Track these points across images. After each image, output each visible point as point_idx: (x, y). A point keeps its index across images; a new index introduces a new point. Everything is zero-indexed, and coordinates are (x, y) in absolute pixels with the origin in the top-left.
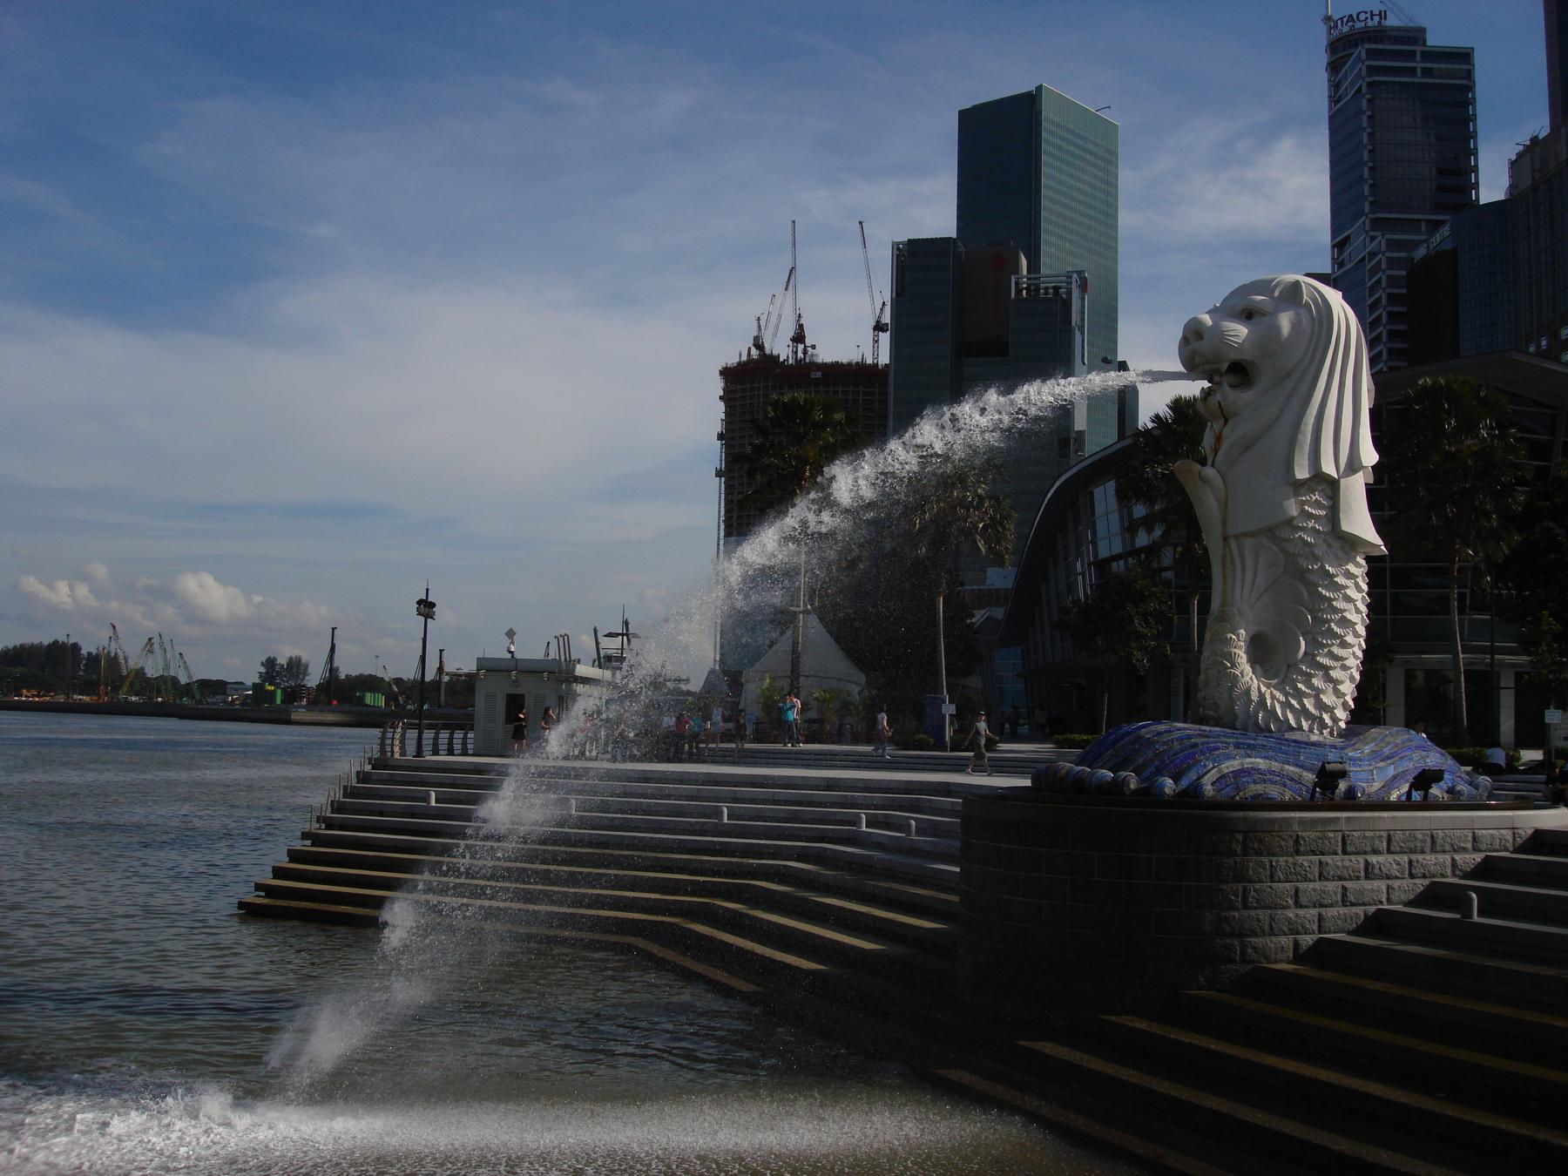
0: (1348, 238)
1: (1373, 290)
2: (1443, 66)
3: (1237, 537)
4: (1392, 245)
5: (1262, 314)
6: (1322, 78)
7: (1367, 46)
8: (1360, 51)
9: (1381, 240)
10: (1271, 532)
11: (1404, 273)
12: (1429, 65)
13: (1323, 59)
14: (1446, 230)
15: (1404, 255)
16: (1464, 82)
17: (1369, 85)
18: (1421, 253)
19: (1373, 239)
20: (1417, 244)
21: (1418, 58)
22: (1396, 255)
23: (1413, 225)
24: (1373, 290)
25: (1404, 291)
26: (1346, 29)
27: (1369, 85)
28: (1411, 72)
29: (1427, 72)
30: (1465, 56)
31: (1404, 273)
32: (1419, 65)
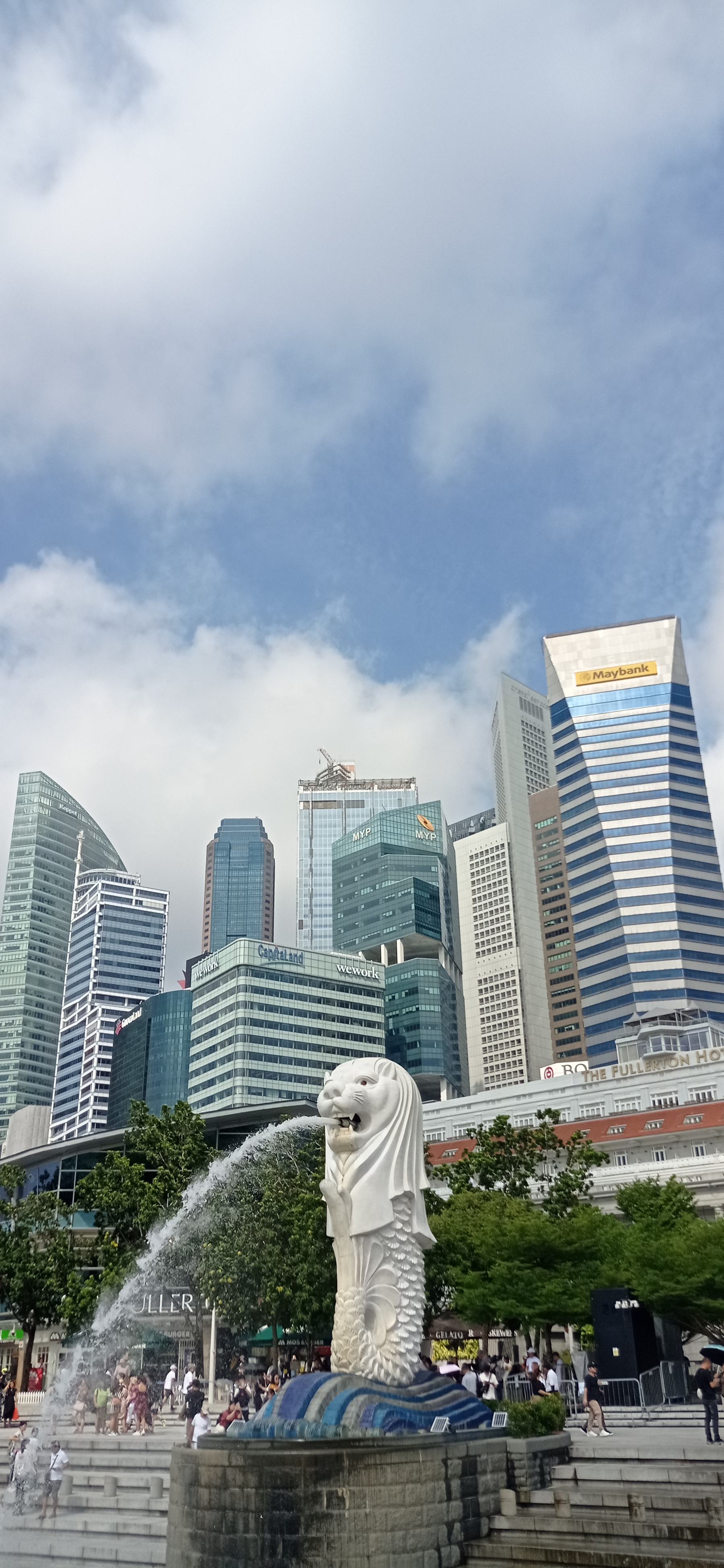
0: (75, 1005)
1: (90, 1041)
3: (357, 1236)
4: (106, 1012)
8: (99, 883)
9: (100, 1006)
10: (376, 1232)
11: (112, 1032)
15: (113, 1020)
16: (162, 912)
17: (102, 906)
19: (92, 1008)
20: (126, 1015)
24: (90, 1041)
25: (111, 1045)
27: (102, 906)
28: (129, 901)
30: (163, 897)
32: (134, 898)
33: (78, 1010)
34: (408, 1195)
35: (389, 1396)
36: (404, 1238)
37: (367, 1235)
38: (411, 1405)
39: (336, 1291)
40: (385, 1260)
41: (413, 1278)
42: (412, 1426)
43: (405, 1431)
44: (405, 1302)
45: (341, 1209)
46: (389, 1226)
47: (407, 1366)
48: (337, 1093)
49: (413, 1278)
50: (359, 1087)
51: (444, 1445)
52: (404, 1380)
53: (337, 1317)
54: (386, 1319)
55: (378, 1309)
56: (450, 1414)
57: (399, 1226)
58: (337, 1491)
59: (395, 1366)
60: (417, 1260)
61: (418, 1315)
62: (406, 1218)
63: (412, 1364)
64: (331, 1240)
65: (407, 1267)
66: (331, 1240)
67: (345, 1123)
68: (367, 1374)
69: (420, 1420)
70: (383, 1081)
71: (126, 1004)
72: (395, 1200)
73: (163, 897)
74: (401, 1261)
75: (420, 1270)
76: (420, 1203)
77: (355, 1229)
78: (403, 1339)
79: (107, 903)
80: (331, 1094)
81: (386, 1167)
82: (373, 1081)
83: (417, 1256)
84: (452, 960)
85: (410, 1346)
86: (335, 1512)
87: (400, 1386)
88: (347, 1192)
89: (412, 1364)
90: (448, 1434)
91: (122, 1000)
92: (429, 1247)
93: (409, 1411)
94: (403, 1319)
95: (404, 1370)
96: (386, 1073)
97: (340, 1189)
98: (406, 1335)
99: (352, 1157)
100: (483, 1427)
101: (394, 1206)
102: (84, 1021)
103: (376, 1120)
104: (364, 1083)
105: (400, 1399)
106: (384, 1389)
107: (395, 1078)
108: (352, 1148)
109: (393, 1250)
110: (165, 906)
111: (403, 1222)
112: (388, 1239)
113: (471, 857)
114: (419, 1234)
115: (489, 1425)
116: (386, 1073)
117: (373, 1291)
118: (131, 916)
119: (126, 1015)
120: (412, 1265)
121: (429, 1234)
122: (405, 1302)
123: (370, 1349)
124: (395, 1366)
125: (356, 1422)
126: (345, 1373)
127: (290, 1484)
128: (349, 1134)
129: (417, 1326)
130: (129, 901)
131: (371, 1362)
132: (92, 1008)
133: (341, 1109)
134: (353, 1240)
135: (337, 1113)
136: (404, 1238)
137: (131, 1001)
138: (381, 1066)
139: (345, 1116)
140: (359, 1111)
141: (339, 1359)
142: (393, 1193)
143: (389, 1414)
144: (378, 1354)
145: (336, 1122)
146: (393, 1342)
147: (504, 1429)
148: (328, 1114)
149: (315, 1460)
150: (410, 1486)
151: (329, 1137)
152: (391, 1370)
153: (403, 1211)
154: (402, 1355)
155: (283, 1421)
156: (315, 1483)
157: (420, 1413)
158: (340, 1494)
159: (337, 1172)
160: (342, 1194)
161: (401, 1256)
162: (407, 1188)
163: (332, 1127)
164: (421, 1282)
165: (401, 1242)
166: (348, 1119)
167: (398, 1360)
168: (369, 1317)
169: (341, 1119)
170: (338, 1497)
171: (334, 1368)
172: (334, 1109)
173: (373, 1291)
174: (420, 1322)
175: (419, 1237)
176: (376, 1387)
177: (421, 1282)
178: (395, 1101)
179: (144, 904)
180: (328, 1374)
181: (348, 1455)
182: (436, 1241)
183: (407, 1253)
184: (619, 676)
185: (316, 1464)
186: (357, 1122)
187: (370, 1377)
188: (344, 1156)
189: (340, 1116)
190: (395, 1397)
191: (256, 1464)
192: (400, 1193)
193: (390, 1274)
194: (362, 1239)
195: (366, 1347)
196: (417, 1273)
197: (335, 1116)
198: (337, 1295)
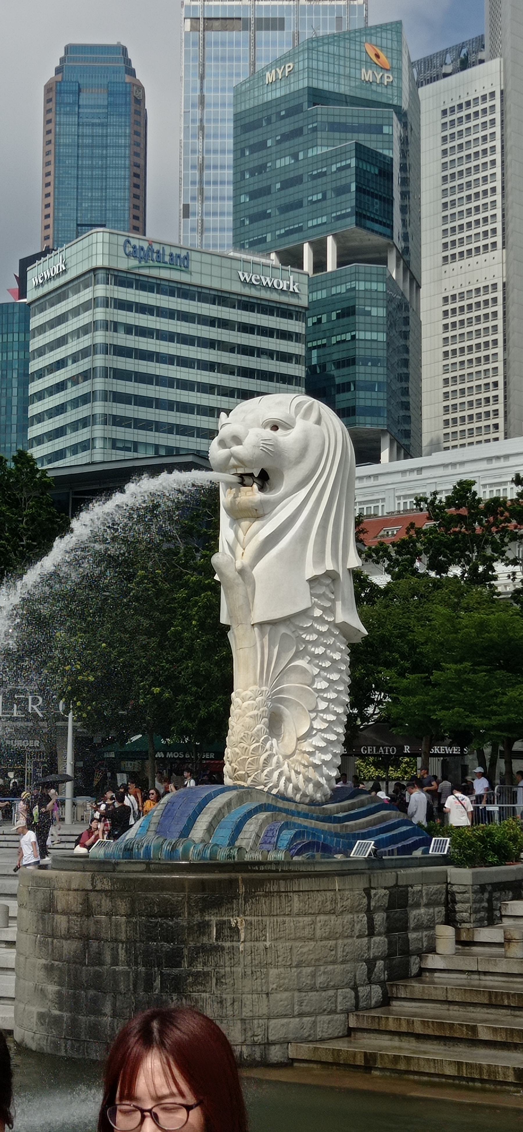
34: (331, 576)
35: (299, 814)
36: (324, 629)
37: (273, 623)
38: (326, 826)
39: (232, 690)
40: (297, 655)
41: (335, 677)
42: (326, 849)
43: (318, 855)
44: (323, 705)
45: (240, 591)
46: (305, 613)
47: (323, 781)
48: (237, 440)
49: (335, 677)
50: (268, 433)
51: (367, 871)
52: (318, 796)
53: (232, 721)
54: (296, 724)
55: (286, 711)
56: (377, 838)
57: (317, 613)
58: (230, 922)
59: (308, 780)
60: (340, 655)
61: (338, 721)
62: (328, 604)
63: (329, 779)
64: (228, 628)
65: (327, 664)
66: (228, 628)
67: (247, 480)
68: (271, 788)
69: (338, 843)
70: (300, 425)
72: (313, 581)
74: (318, 656)
75: (344, 667)
76: (347, 586)
77: (258, 615)
78: (318, 748)
80: (228, 441)
81: (303, 539)
82: (288, 426)
83: (341, 651)
84: (407, 267)
85: (328, 757)
86: (227, 944)
87: (313, 803)
88: (248, 569)
89: (329, 779)
90: (373, 860)
92: (358, 640)
93: (323, 832)
94: (318, 725)
95: (318, 786)
96: (306, 416)
97: (239, 564)
98: (323, 744)
99: (256, 524)
100: (418, 853)
101: (311, 588)
103: (290, 478)
104: (275, 428)
105: (312, 818)
106: (292, 807)
107: (318, 422)
108: (257, 513)
109: (309, 642)
111: (324, 609)
112: (303, 629)
114: (344, 623)
115: (426, 851)
116: (306, 416)
117: (281, 691)
120: (334, 661)
121: (357, 623)
122: (323, 705)
123: (274, 760)
124: (308, 780)
125: (255, 843)
126: (243, 787)
127: (170, 911)
128: (252, 494)
129: (338, 734)
131: (276, 774)
133: (242, 462)
134: (256, 629)
135: (235, 467)
136: (324, 629)
138: (299, 405)
139: (248, 471)
140: (266, 466)
141: (235, 770)
142: (310, 572)
143: (296, 836)
144: (286, 766)
145: (235, 479)
146: (305, 752)
147: (444, 856)
148: (224, 467)
149: (202, 885)
150: (322, 918)
151: (225, 498)
152: (301, 784)
153: (324, 594)
154: (316, 767)
155: (161, 840)
156: (202, 911)
157: (337, 835)
158: (233, 924)
159: (234, 545)
160: (242, 572)
161: (320, 650)
162: (329, 565)
163: (229, 485)
164: (344, 682)
165: (321, 634)
166: (251, 475)
167: (311, 773)
168: (274, 723)
169: (241, 476)
170: (231, 928)
171: (228, 781)
172: (233, 461)
173: (281, 691)
174: (341, 730)
175: (344, 629)
176: (281, 804)
177: (344, 682)
178: (317, 453)
180: (220, 787)
181: (244, 880)
182: (367, 633)
183: (327, 646)
185: (203, 890)
186: (264, 480)
187: (274, 791)
188: (245, 524)
189: (240, 471)
190: (306, 816)
191: (127, 888)
192: (320, 572)
193: (304, 671)
194: (268, 628)
195: (270, 756)
196: (340, 671)
197: (234, 471)
198: (233, 694)
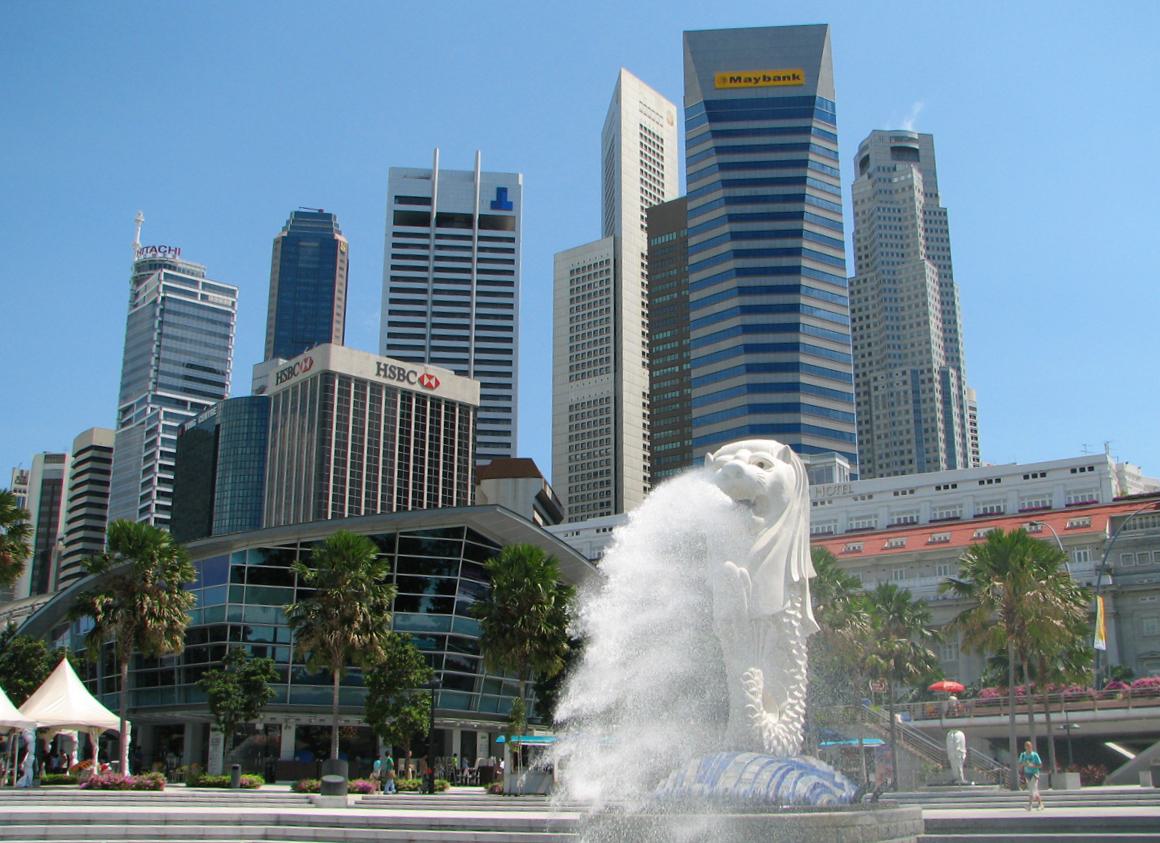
0: (132, 406)
2: (216, 295)
4: (165, 413)
5: (770, 465)
6: (126, 288)
7: (165, 271)
11: (175, 437)
12: (205, 293)
13: (131, 273)
14: (212, 412)
15: (176, 425)
16: (229, 309)
17: (163, 298)
18: (190, 425)
21: (200, 287)
22: (168, 423)
23: (182, 404)
25: (174, 451)
26: (149, 255)
28: (194, 295)
29: (204, 297)
30: (232, 293)
31: (175, 437)
32: (200, 291)
33: (137, 411)
71: (189, 408)
73: (232, 293)
79: (168, 295)
91: (182, 404)
102: (143, 423)
104: (761, 465)
110: (233, 303)
113: (572, 272)
118: (195, 312)
119: (189, 419)
130: (194, 295)
132: (152, 409)
137: (193, 404)
179: (211, 299)
184: (761, 83)
